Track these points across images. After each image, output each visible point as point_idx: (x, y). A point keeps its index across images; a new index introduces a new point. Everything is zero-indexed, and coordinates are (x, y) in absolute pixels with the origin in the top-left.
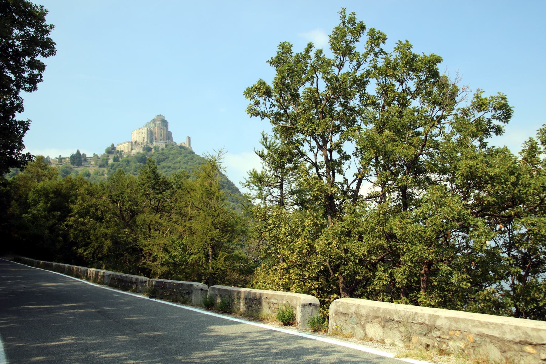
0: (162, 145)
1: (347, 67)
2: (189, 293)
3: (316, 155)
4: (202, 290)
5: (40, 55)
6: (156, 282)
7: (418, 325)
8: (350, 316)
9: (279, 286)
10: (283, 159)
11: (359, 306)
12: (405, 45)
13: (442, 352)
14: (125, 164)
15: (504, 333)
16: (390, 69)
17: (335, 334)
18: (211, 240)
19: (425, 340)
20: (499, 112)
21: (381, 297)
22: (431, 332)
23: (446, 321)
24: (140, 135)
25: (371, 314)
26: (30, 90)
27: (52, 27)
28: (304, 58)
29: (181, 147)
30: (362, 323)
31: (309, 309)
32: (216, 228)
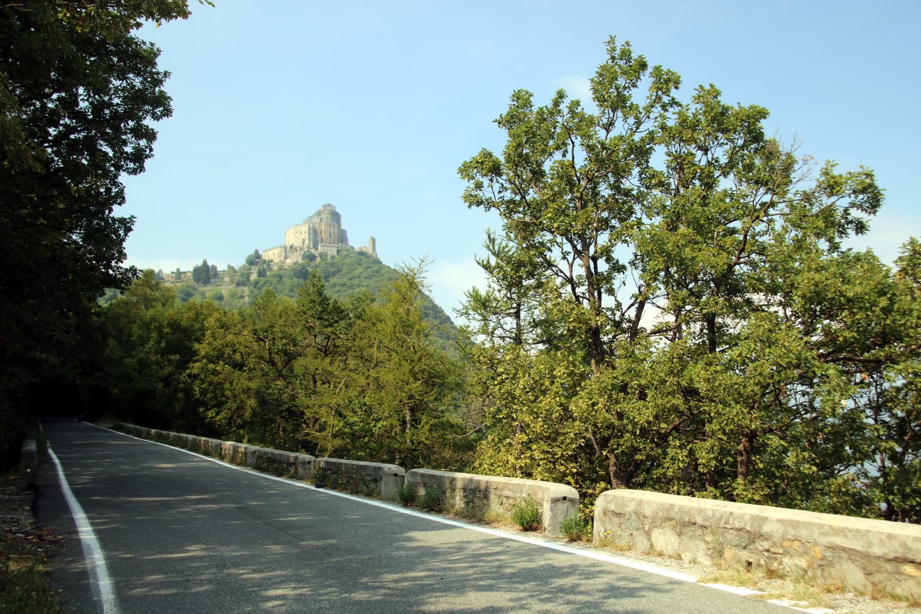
0: (332, 251)
1: (620, 128)
2: (376, 481)
3: (571, 266)
4: (396, 475)
5: (149, 117)
6: (326, 462)
7: (735, 532)
8: (627, 517)
9: (515, 469)
10: (520, 272)
11: (640, 502)
12: (708, 91)
13: (771, 574)
14: (275, 280)
15: (870, 544)
16: (687, 129)
17: (605, 544)
18: (409, 399)
19: (745, 555)
20: (861, 196)
21: (675, 488)
22: (754, 542)
23: (779, 525)
24: (298, 237)
25: (660, 515)
26: (134, 172)
27: (166, 74)
28: (552, 114)
29: (361, 253)
30: (646, 528)
31: (563, 506)
32: (416, 379)
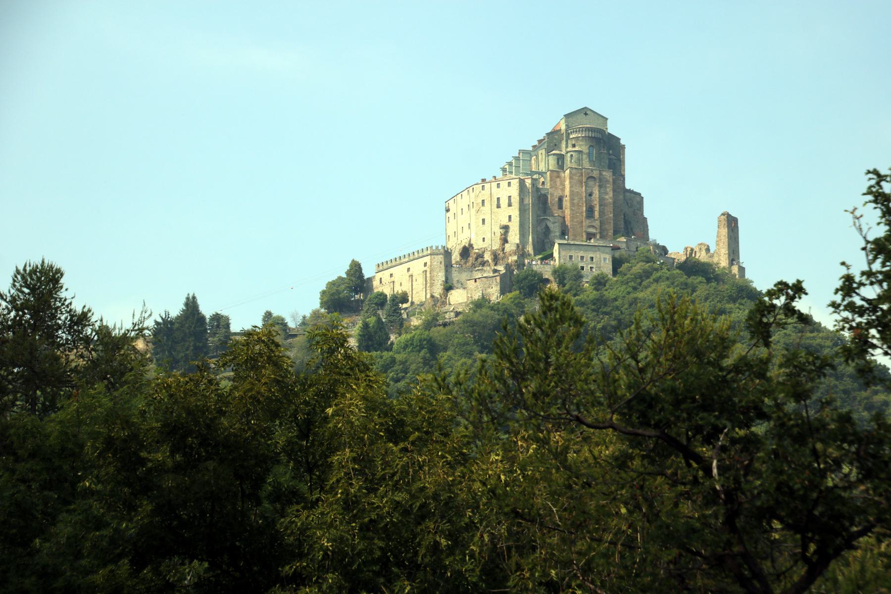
0: (597, 262)
14: (416, 359)
29: (694, 268)
